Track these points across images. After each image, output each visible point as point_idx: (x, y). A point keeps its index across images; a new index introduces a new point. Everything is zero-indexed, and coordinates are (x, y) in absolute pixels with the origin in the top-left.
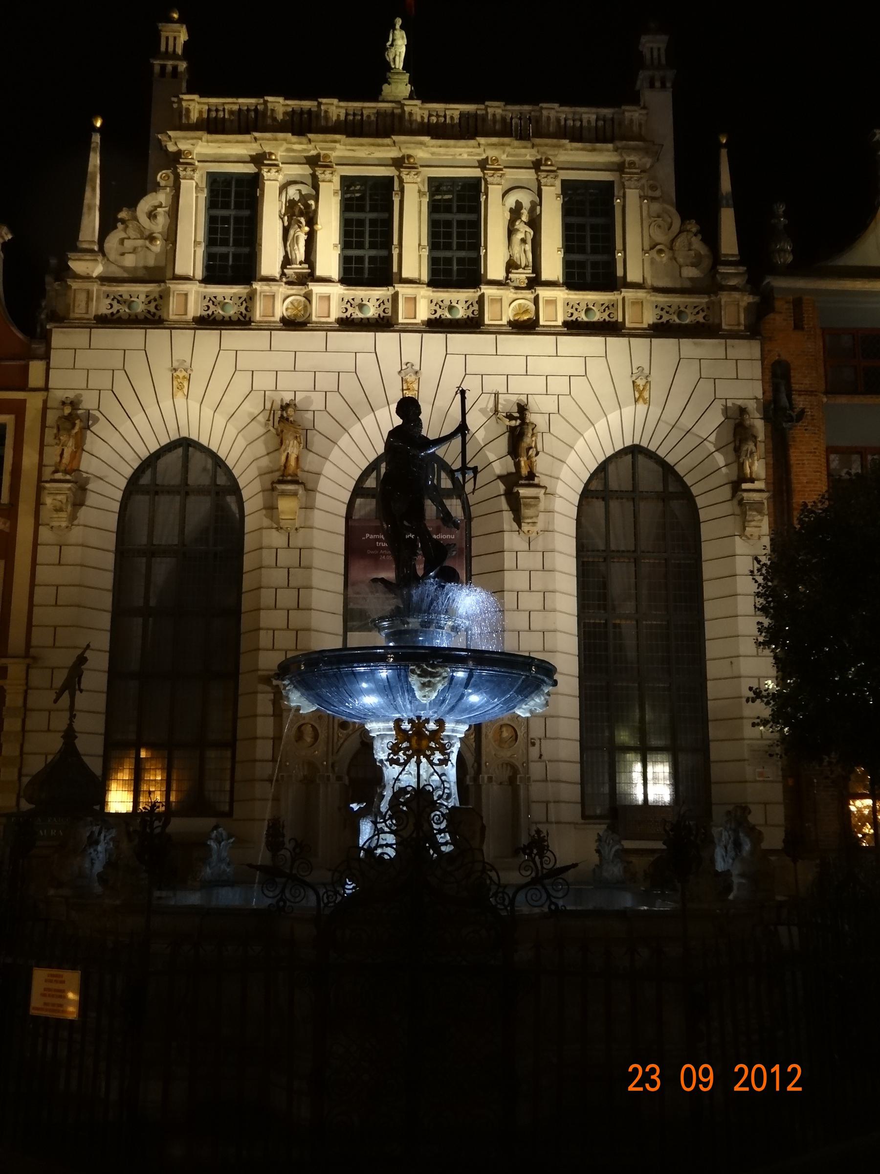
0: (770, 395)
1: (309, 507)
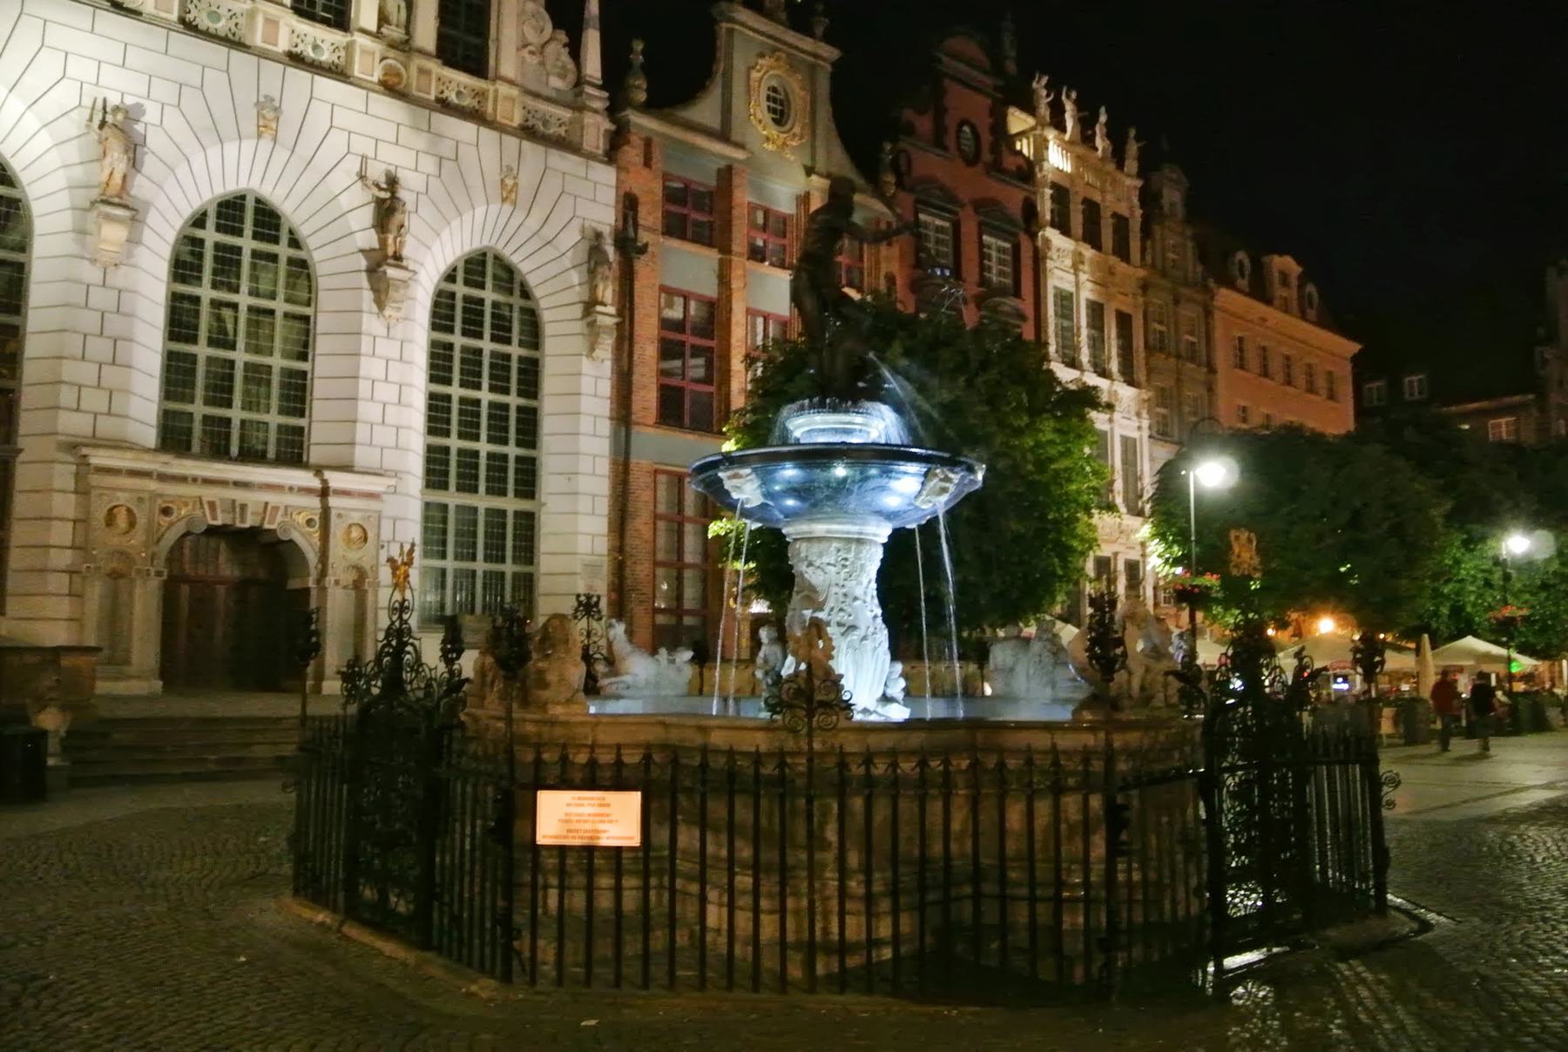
0: (620, 223)
1: (134, 240)
